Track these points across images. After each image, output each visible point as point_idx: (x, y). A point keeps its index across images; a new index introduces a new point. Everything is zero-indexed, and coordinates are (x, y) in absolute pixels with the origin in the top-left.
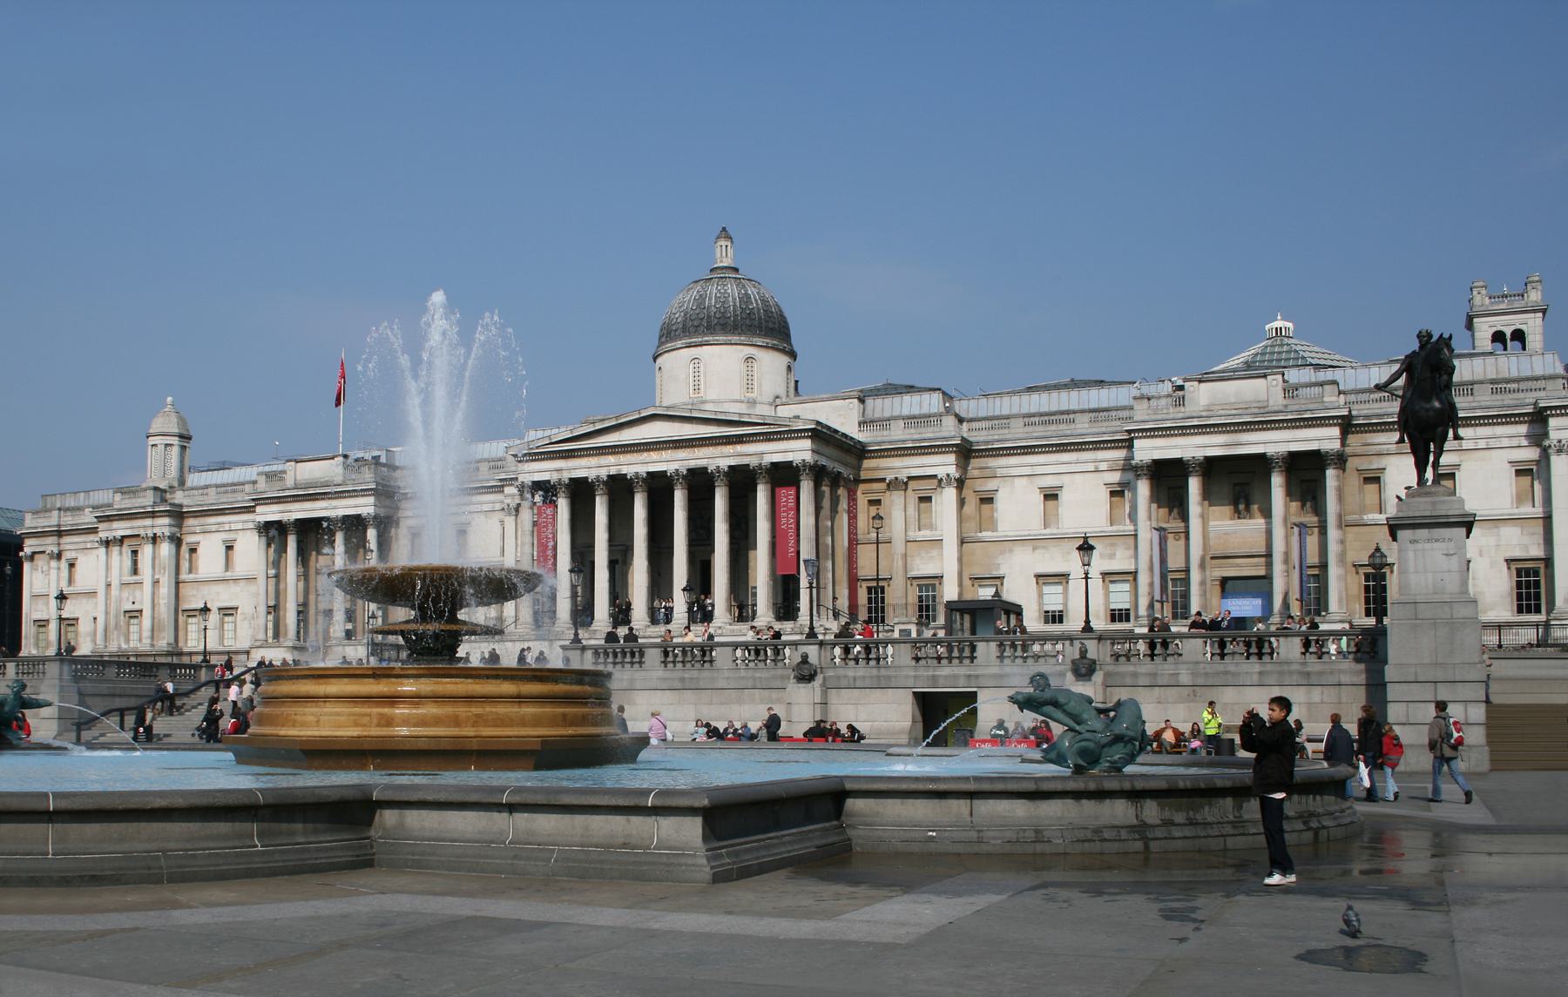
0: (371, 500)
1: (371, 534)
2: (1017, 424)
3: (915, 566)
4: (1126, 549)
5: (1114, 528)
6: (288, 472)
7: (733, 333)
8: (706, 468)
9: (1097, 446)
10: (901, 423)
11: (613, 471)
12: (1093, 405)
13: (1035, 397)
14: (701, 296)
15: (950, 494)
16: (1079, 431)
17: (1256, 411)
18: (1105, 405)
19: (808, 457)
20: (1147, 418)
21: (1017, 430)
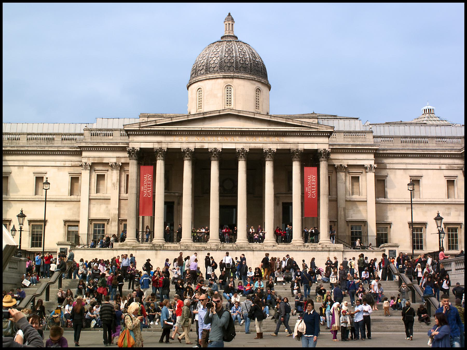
3: (350, 215)
7: (251, 73)
9: (441, 156)
10: (343, 134)
11: (198, 146)
12: (434, 135)
13: (391, 127)
14: (229, 49)
16: (430, 148)
18: (443, 135)
21: (397, 144)
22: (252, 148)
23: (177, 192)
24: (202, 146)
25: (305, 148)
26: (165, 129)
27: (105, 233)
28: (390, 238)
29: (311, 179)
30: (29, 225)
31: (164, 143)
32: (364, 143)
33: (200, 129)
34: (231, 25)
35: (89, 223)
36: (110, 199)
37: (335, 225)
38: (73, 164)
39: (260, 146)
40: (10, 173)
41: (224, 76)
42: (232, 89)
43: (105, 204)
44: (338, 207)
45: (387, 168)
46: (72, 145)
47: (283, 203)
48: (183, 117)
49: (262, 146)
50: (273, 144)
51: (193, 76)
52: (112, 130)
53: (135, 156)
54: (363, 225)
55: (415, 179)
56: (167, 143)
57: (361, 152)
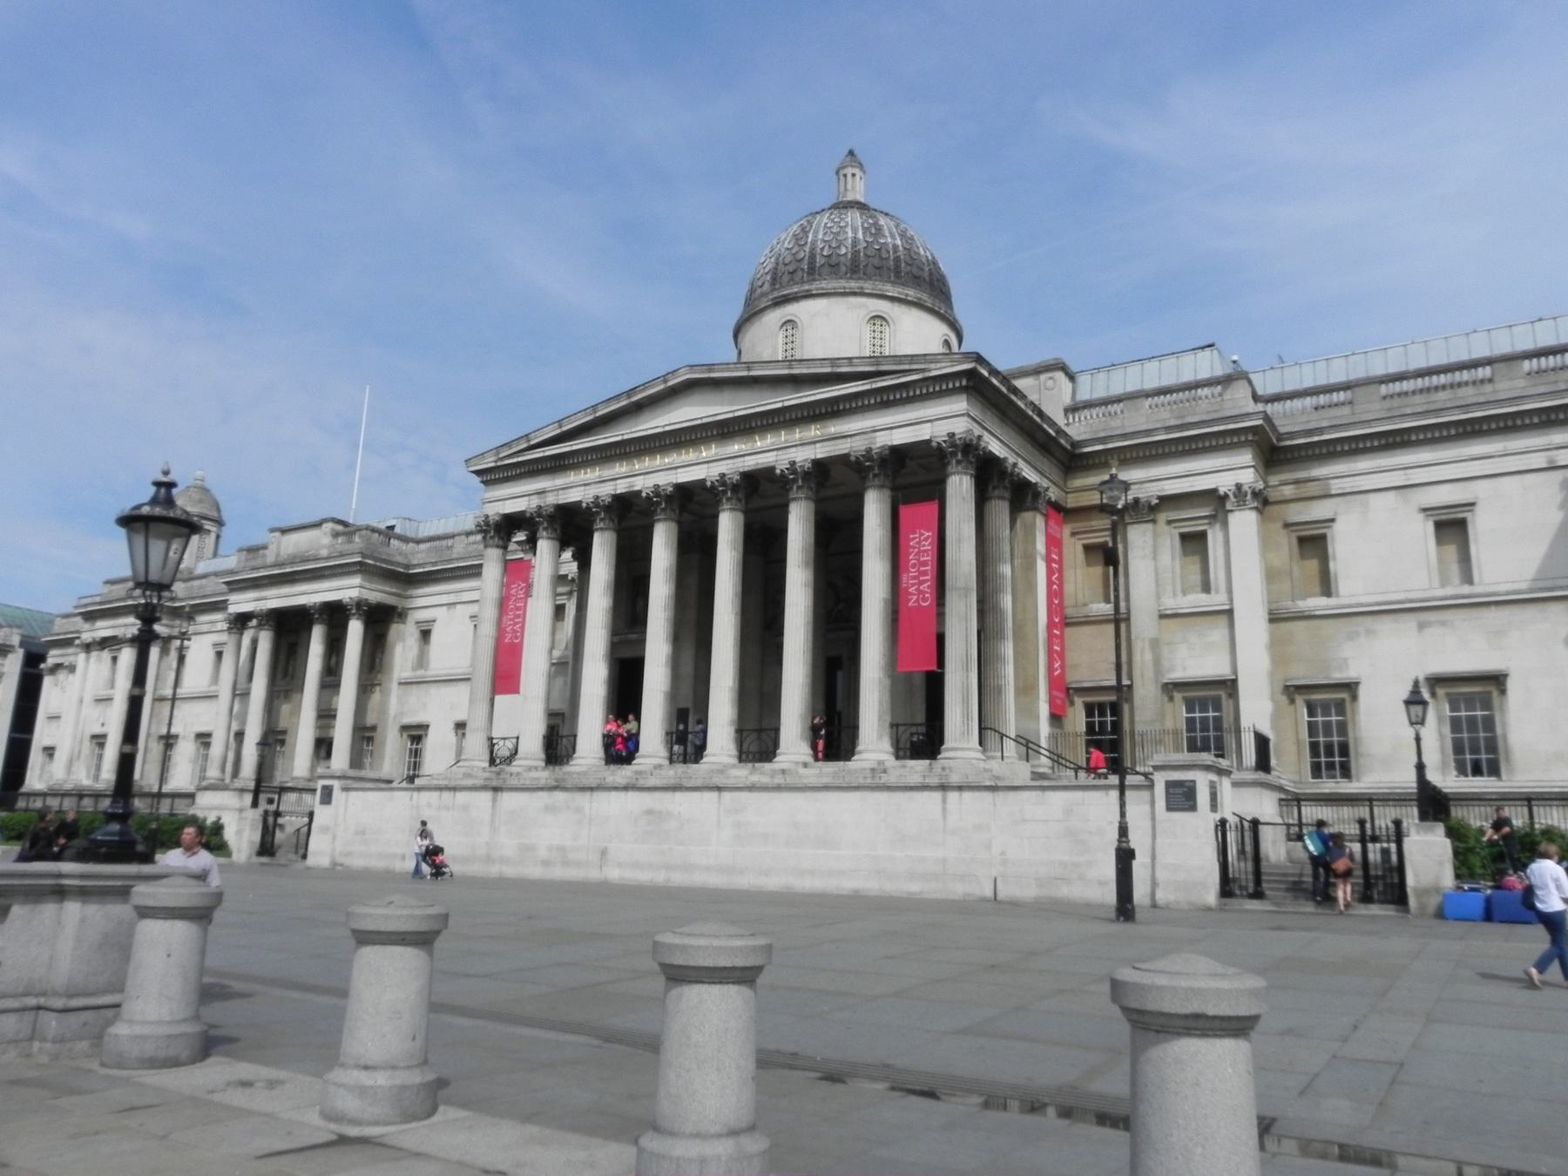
0: (357, 580)
1: (355, 629)
7: (851, 278)
8: (773, 468)
11: (621, 487)
19: (960, 427)
22: (750, 469)
24: (629, 487)
25: (895, 443)
28: (1356, 739)
29: (919, 543)
31: (550, 494)
39: (771, 459)
40: (434, 621)
41: (776, 298)
44: (1133, 637)
45: (1333, 492)
48: (583, 413)
49: (774, 459)
54: (1222, 694)
55: (1444, 517)
57: (915, 395)
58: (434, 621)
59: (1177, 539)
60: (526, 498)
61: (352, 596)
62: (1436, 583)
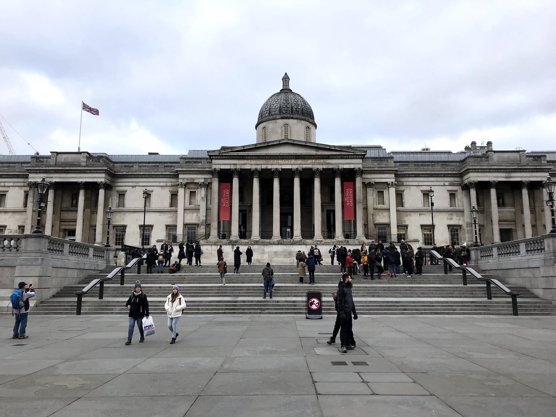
0: (103, 175)
1: (102, 192)
2: (412, 166)
3: (377, 219)
4: (457, 216)
5: (452, 208)
6: (52, 158)
7: (302, 116)
9: (445, 176)
10: (371, 160)
11: (264, 167)
15: (392, 191)
16: (437, 170)
17: (517, 165)
20: (475, 165)
21: (411, 167)
23: (249, 203)
25: (344, 168)
26: (239, 154)
27: (196, 233)
29: (349, 191)
30: (140, 229)
31: (238, 165)
32: (387, 166)
33: (265, 154)
34: (287, 81)
35: (184, 227)
36: (200, 209)
37: (365, 227)
38: (173, 184)
40: (126, 191)
41: (283, 117)
42: (289, 127)
43: (196, 213)
46: (172, 170)
47: (327, 211)
50: (320, 165)
51: (260, 118)
52: (201, 159)
53: (217, 175)
54: (387, 226)
55: (425, 193)
56: (240, 165)
58: (126, 191)
59: (377, 192)
60: (230, 165)
61: (102, 181)
62: (423, 206)
